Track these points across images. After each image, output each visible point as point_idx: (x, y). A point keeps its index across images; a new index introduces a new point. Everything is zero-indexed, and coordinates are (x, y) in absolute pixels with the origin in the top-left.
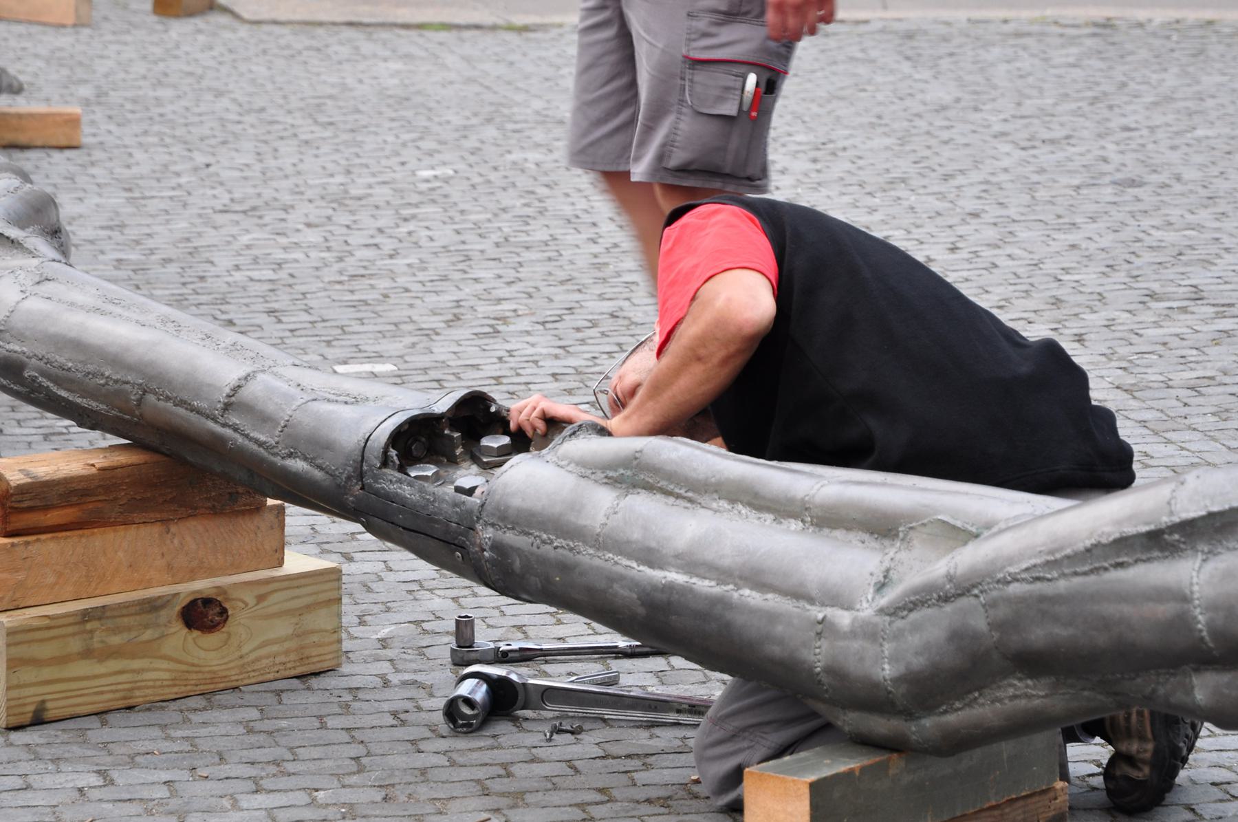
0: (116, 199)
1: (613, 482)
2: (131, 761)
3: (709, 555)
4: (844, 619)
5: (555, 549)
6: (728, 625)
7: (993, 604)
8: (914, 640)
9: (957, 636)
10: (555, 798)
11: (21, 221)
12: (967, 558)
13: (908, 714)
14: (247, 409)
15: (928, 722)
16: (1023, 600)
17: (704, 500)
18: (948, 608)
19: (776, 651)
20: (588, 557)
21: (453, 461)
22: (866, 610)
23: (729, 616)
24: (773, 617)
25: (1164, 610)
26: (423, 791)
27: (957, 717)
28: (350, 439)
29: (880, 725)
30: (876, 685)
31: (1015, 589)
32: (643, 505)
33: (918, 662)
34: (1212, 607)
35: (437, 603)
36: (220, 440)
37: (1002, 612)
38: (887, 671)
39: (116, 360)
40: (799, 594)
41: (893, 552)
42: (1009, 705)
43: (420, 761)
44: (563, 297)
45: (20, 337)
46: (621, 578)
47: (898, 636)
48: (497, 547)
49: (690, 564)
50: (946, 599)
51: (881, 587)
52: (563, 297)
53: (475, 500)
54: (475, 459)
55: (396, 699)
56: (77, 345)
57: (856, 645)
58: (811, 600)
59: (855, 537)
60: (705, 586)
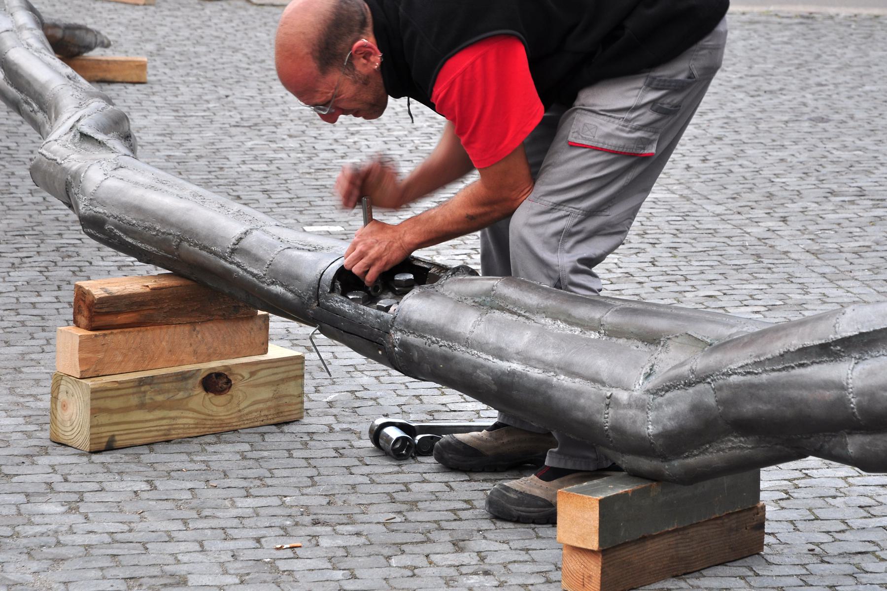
0: (168, 117)
2: (169, 475)
4: (623, 396)
5: (440, 347)
6: (549, 398)
7: (720, 388)
8: (669, 410)
9: (696, 408)
10: (437, 505)
11: (105, 130)
13: (664, 458)
14: (246, 253)
15: (676, 463)
16: (738, 386)
18: (691, 390)
19: (580, 415)
20: (461, 353)
23: (550, 392)
24: (578, 394)
25: (830, 395)
26: (353, 499)
27: (694, 460)
28: (310, 274)
29: (646, 464)
30: (643, 439)
31: (734, 379)
33: (671, 425)
34: (860, 393)
35: (365, 380)
36: (229, 272)
37: (725, 394)
38: (651, 429)
39: (163, 221)
40: (595, 380)
42: (729, 453)
43: (351, 480)
45: (103, 204)
47: (659, 407)
48: (404, 344)
49: (526, 360)
50: (689, 384)
51: (648, 376)
55: (337, 440)
56: (139, 209)
57: (631, 412)
58: (603, 384)
60: (535, 373)
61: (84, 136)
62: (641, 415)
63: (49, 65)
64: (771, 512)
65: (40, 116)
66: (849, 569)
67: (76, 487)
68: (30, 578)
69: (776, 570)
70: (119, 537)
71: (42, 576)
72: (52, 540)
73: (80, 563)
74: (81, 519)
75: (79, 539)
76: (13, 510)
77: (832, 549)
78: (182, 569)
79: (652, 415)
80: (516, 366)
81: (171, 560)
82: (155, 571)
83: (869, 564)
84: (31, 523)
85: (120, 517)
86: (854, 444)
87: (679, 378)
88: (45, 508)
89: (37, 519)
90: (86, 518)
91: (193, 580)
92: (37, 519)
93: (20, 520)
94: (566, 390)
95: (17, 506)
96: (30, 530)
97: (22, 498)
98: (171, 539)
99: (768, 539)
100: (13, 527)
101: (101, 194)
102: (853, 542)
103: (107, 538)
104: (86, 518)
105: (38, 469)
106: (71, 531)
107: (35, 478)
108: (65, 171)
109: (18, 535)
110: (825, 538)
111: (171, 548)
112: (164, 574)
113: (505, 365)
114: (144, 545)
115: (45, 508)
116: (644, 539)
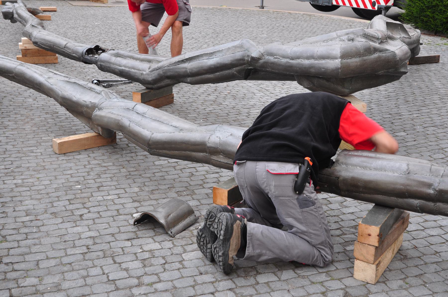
0: (55, 27)
1: (115, 56)
3: (128, 65)
4: (144, 73)
5: (108, 65)
6: (130, 74)
7: (163, 70)
8: (153, 75)
9: (159, 74)
11: (38, 25)
12: (160, 65)
13: (153, 84)
14: (67, 48)
15: (156, 86)
16: (167, 69)
17: (127, 58)
18: (157, 71)
19: (136, 77)
20: (112, 66)
21: (95, 54)
22: (147, 72)
23: (130, 73)
24: (136, 73)
25: (184, 70)
27: (159, 85)
29: (150, 86)
30: (149, 81)
31: (166, 68)
32: (119, 59)
33: (154, 78)
34: (190, 69)
35: (95, 74)
36: (64, 52)
37: (164, 71)
38: (150, 79)
39: (50, 42)
40: (139, 70)
41: (151, 64)
42: (165, 83)
44: (113, 38)
45: (37, 39)
46: (116, 68)
47: (152, 74)
48: (100, 65)
49: (125, 67)
50: (157, 70)
51: (149, 69)
52: (113, 38)
53: (97, 59)
54: (98, 54)
56: (44, 40)
57: (146, 76)
58: (140, 71)
59: (146, 62)
60: (127, 69)
61: (33, 26)
62: (148, 76)
63: (26, 13)
64: (175, 95)
65: (25, 23)
66: (190, 105)
67: (35, 96)
68: (26, 113)
69: (176, 106)
70: (44, 105)
71: (28, 113)
72: (30, 106)
73: (36, 110)
74: (36, 102)
75: (36, 106)
76: (22, 101)
77: (187, 102)
79: (150, 76)
80: (123, 68)
81: (55, 109)
82: (52, 111)
84: (26, 103)
85: (45, 101)
86: (189, 79)
87: (155, 68)
88: (29, 100)
89: (27, 102)
90: (37, 101)
91: (59, 113)
92: (27, 102)
93: (23, 102)
94: (133, 72)
95: (23, 100)
96: (26, 104)
97: (24, 98)
98: (55, 105)
99: (174, 100)
100: (22, 104)
101: (36, 37)
102: (191, 100)
103: (42, 105)
104: (37, 101)
105: (27, 93)
106: (34, 104)
107: (27, 95)
108: (29, 33)
109: (23, 105)
110: (186, 100)
111: (55, 107)
112: (53, 112)
113: (121, 68)
114: (49, 106)
115: (29, 100)
116: (150, 101)
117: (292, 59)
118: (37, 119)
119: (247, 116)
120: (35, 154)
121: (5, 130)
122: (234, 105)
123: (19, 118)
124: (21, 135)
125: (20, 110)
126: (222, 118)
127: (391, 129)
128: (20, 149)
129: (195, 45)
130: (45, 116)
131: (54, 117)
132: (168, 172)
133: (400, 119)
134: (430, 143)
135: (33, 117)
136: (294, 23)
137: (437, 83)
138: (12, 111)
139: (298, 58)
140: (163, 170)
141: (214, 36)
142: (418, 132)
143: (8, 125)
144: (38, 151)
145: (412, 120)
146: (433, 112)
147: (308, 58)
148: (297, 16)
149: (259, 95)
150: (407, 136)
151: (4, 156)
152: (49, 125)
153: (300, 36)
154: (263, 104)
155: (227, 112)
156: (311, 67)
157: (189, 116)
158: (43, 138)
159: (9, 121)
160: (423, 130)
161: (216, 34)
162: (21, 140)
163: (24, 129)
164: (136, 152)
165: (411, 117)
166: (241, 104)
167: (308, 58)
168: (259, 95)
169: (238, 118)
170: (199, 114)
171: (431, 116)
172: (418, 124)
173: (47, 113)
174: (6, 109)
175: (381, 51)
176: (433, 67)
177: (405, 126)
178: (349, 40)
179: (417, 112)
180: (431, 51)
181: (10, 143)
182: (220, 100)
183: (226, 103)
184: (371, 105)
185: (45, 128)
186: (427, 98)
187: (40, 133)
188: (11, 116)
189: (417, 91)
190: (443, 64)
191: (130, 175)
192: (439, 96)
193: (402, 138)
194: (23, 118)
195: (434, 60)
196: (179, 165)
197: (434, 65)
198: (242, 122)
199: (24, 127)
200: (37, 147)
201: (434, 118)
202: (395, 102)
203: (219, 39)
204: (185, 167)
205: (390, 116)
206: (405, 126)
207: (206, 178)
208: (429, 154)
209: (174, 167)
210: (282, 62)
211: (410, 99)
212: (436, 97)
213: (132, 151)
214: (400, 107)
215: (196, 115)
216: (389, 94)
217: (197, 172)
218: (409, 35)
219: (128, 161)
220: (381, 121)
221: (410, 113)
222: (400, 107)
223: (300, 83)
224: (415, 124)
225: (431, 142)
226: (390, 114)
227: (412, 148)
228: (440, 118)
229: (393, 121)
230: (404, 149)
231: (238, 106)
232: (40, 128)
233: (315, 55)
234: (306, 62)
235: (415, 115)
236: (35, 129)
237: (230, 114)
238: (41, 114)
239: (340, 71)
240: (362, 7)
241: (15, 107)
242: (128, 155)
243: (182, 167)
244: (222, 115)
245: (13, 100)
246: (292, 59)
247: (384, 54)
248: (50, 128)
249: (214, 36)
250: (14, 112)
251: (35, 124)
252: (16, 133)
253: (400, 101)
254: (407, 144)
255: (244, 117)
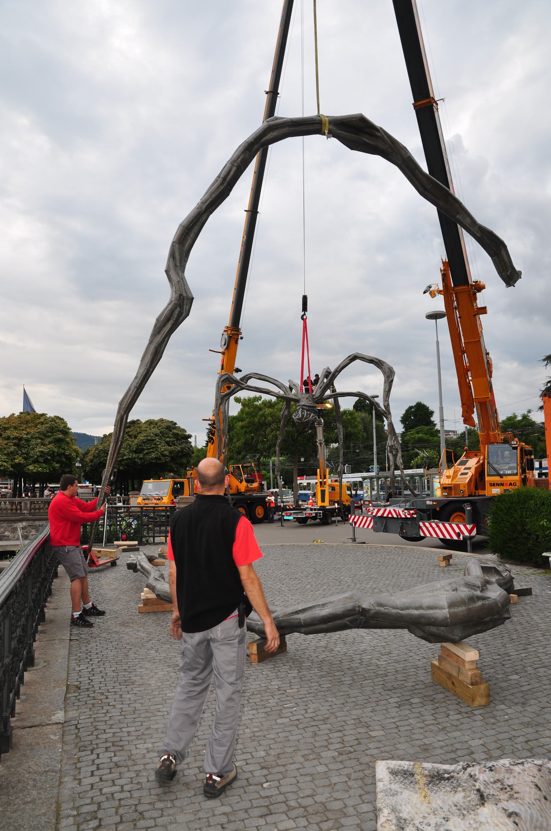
4: (259, 623)
25: (298, 621)
40: (254, 620)
73: (158, 663)
75: (158, 658)
78: (178, 663)
83: (306, 651)
96: (149, 657)
102: (303, 647)
106: (157, 656)
109: (146, 658)
111: (176, 659)
117: (402, 609)
118: (160, 673)
119: (360, 663)
120: (162, 714)
121: (133, 686)
122: (346, 650)
123: (144, 672)
124: (147, 691)
125: (143, 663)
126: (336, 666)
127: (504, 672)
128: (147, 708)
129: (299, 586)
130: (168, 669)
131: (176, 671)
132: (291, 732)
133: (510, 660)
134: (544, 687)
135: (156, 671)
136: (388, 557)
137: (535, 617)
138: (137, 665)
139: (408, 608)
140: (287, 729)
141: (316, 575)
142: (530, 674)
143: (135, 681)
144: (165, 709)
145: (522, 661)
146: (540, 651)
147: (417, 608)
148: (389, 550)
149: (368, 638)
150: (520, 679)
151: (134, 716)
152: (172, 680)
153: (396, 571)
154: (373, 648)
155: (340, 659)
156: (421, 616)
157: (303, 665)
158: (168, 695)
159: (136, 676)
160: (534, 671)
161: (318, 573)
162: (149, 697)
163: (150, 684)
164: (257, 709)
165: (519, 656)
166: (352, 649)
167: (417, 608)
168: (368, 638)
169: (352, 665)
170: (312, 662)
171: (539, 655)
172: (528, 665)
173: (169, 666)
174: (132, 663)
175: (484, 599)
176: (528, 599)
177: (516, 668)
178: (453, 591)
179: (524, 651)
180: (522, 582)
181: (138, 701)
182: (331, 646)
183: (337, 649)
184: (479, 645)
185: (169, 683)
186: (530, 634)
187: (165, 689)
188: (137, 670)
189: (518, 628)
190: (536, 596)
191: (254, 736)
192: (541, 632)
193: (515, 682)
194: (148, 672)
195: (526, 592)
196: (301, 723)
197: (528, 597)
198: (356, 670)
199: (149, 683)
200: (163, 705)
201: (542, 658)
202: (501, 641)
203: (321, 579)
204: (308, 725)
205: (500, 657)
206: (516, 668)
207: (330, 738)
208: (546, 699)
209: (297, 726)
210: (392, 612)
211: (515, 637)
212: (538, 633)
213: (253, 708)
214: (507, 646)
215: (310, 664)
216: (494, 632)
217: (320, 730)
218: (503, 576)
219: (251, 720)
220: (492, 663)
221: (518, 653)
222: (507, 646)
223: (410, 631)
224: (525, 665)
225: (545, 685)
226: (499, 655)
227: (529, 693)
228: (547, 657)
229: (504, 663)
230: (521, 694)
231: (349, 652)
232: (164, 683)
233: (424, 606)
234: (416, 612)
235: (523, 655)
236: (160, 684)
237: (343, 661)
238: (164, 667)
239: (449, 620)
240: (448, 537)
241: (140, 660)
242: (249, 712)
243: (305, 726)
244: (335, 663)
245: (137, 653)
246: (402, 609)
247: (487, 602)
248: (173, 683)
249: (316, 575)
250: (139, 665)
251: (159, 678)
252: (143, 689)
253: (506, 639)
254: (524, 689)
255: (357, 665)
